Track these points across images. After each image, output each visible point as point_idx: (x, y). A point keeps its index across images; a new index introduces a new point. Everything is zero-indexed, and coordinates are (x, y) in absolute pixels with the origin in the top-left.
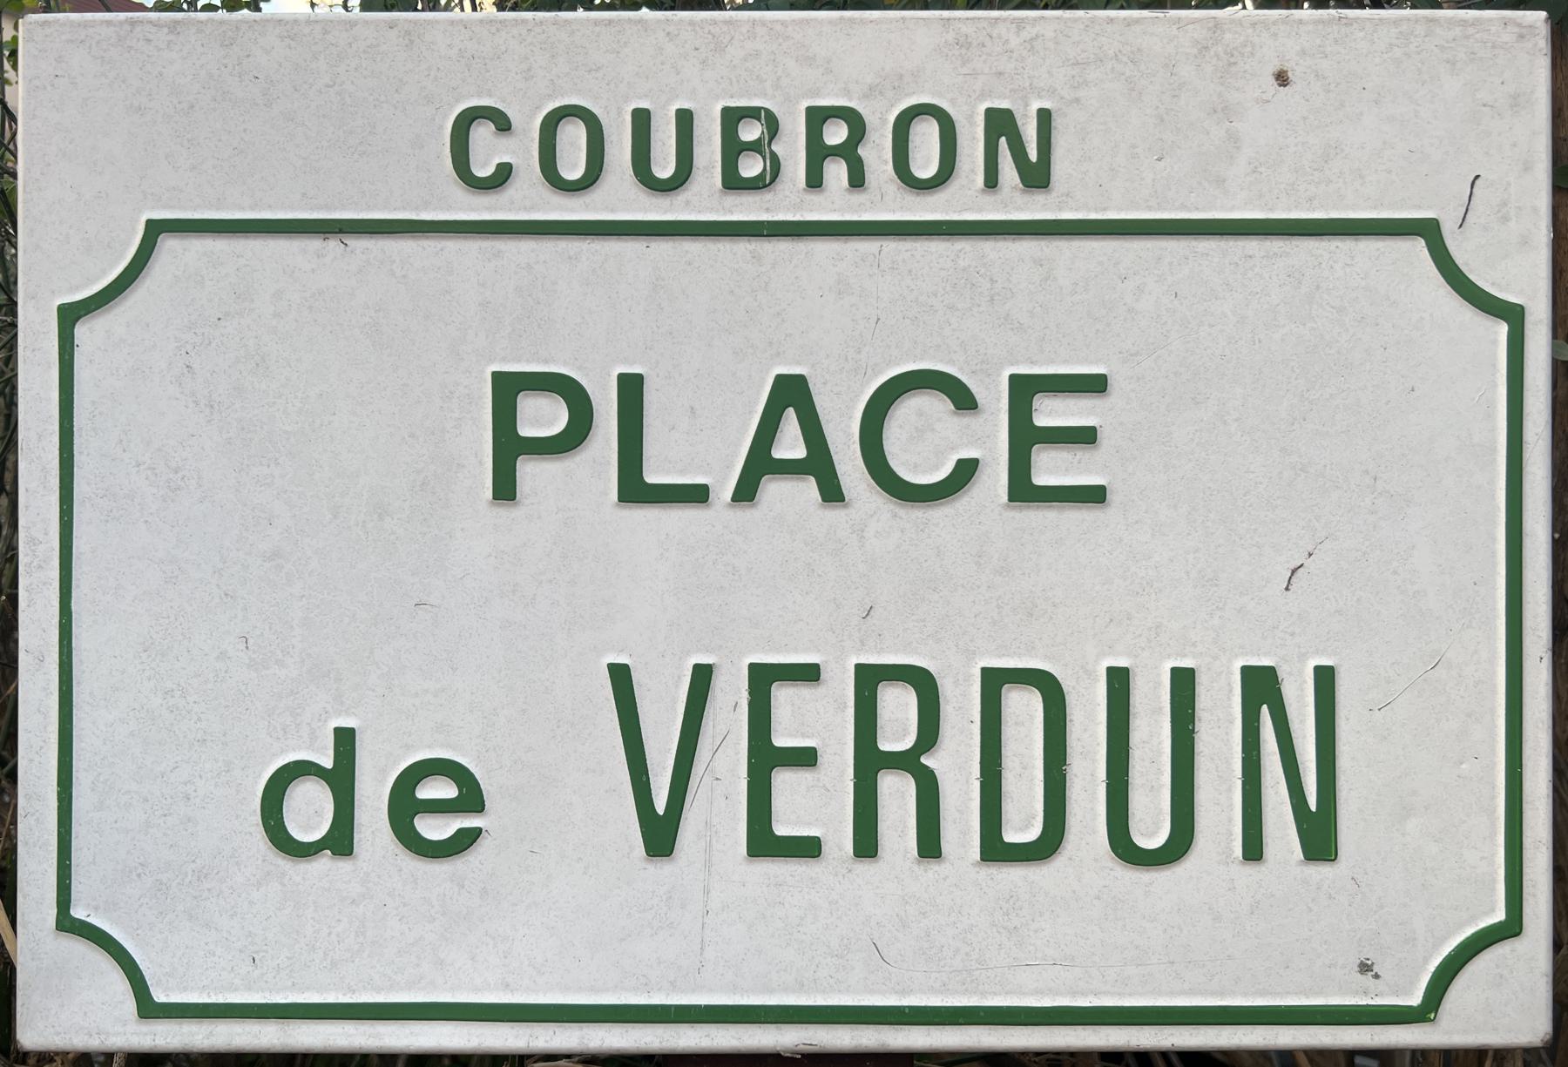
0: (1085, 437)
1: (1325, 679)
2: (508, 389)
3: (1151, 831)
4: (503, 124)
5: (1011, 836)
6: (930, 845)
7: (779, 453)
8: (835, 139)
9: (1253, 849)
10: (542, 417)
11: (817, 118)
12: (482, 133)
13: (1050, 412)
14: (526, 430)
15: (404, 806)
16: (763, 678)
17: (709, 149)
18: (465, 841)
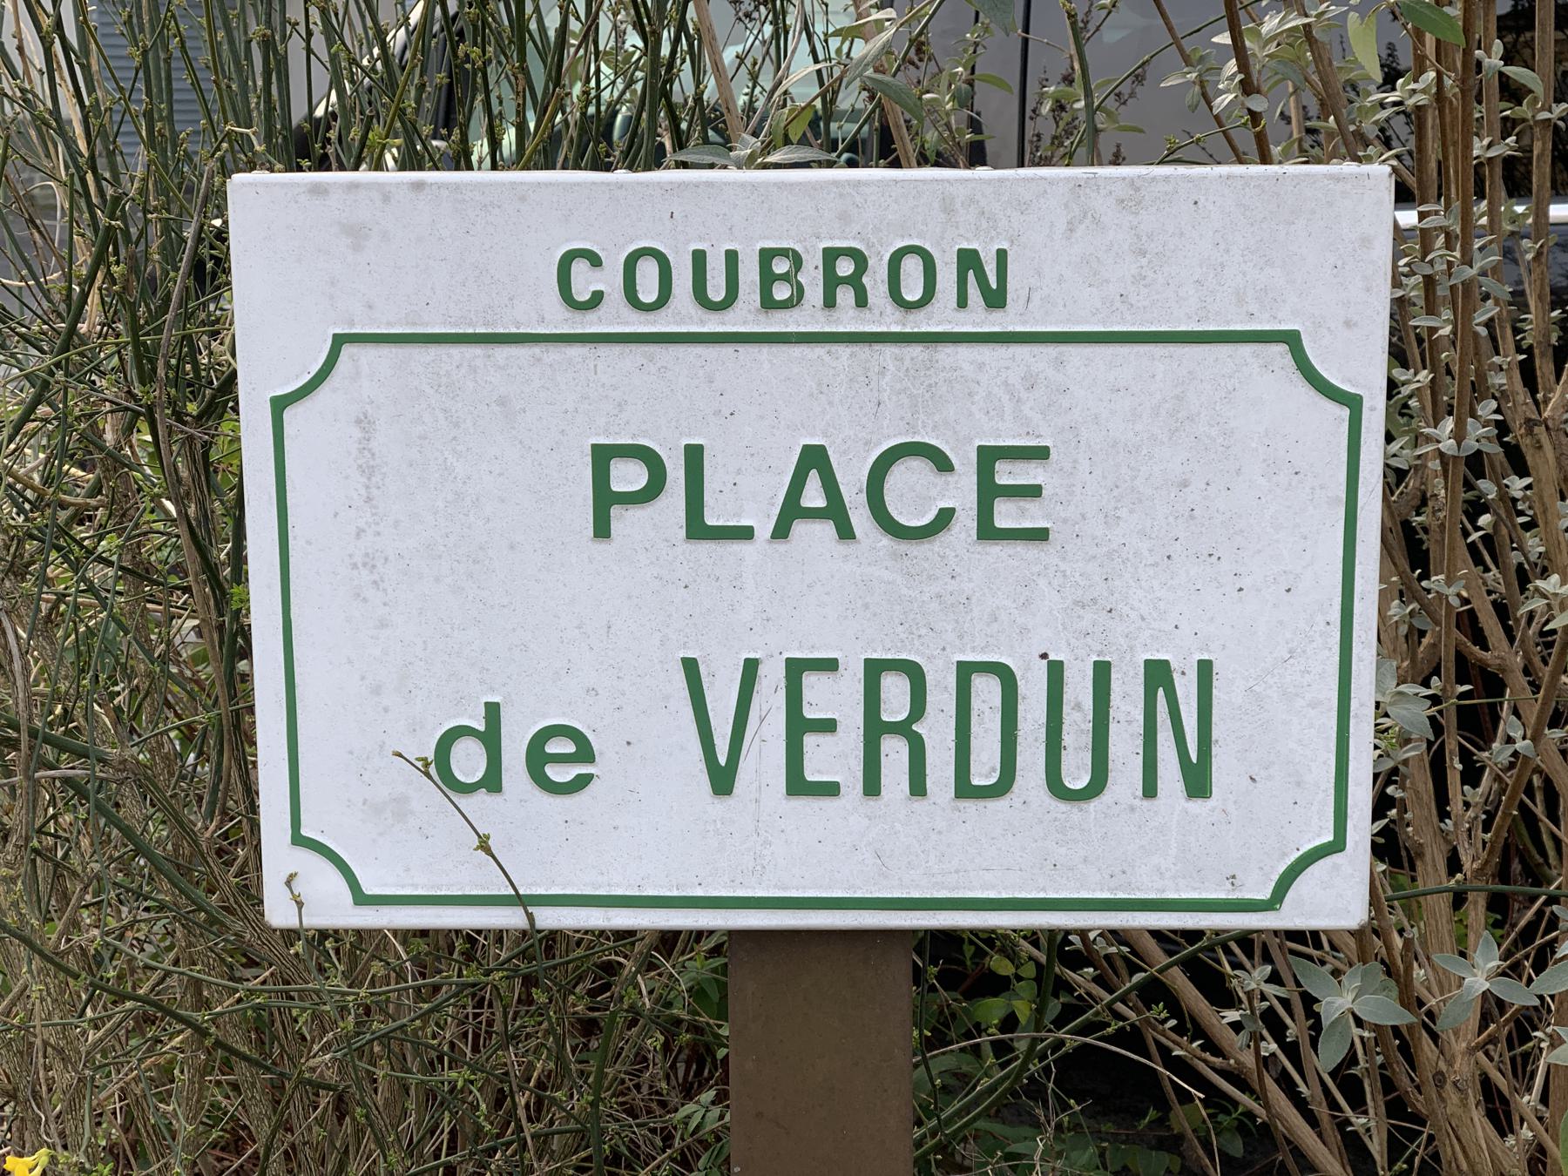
0: (1034, 492)
1: (1205, 669)
2: (603, 457)
3: (1077, 776)
4: (595, 260)
5: (976, 781)
6: (918, 787)
8: (844, 272)
9: (1150, 790)
10: (628, 476)
11: (831, 256)
12: (579, 268)
13: (1006, 474)
14: (616, 486)
15: (537, 758)
16: (796, 669)
17: (749, 274)
18: (582, 782)
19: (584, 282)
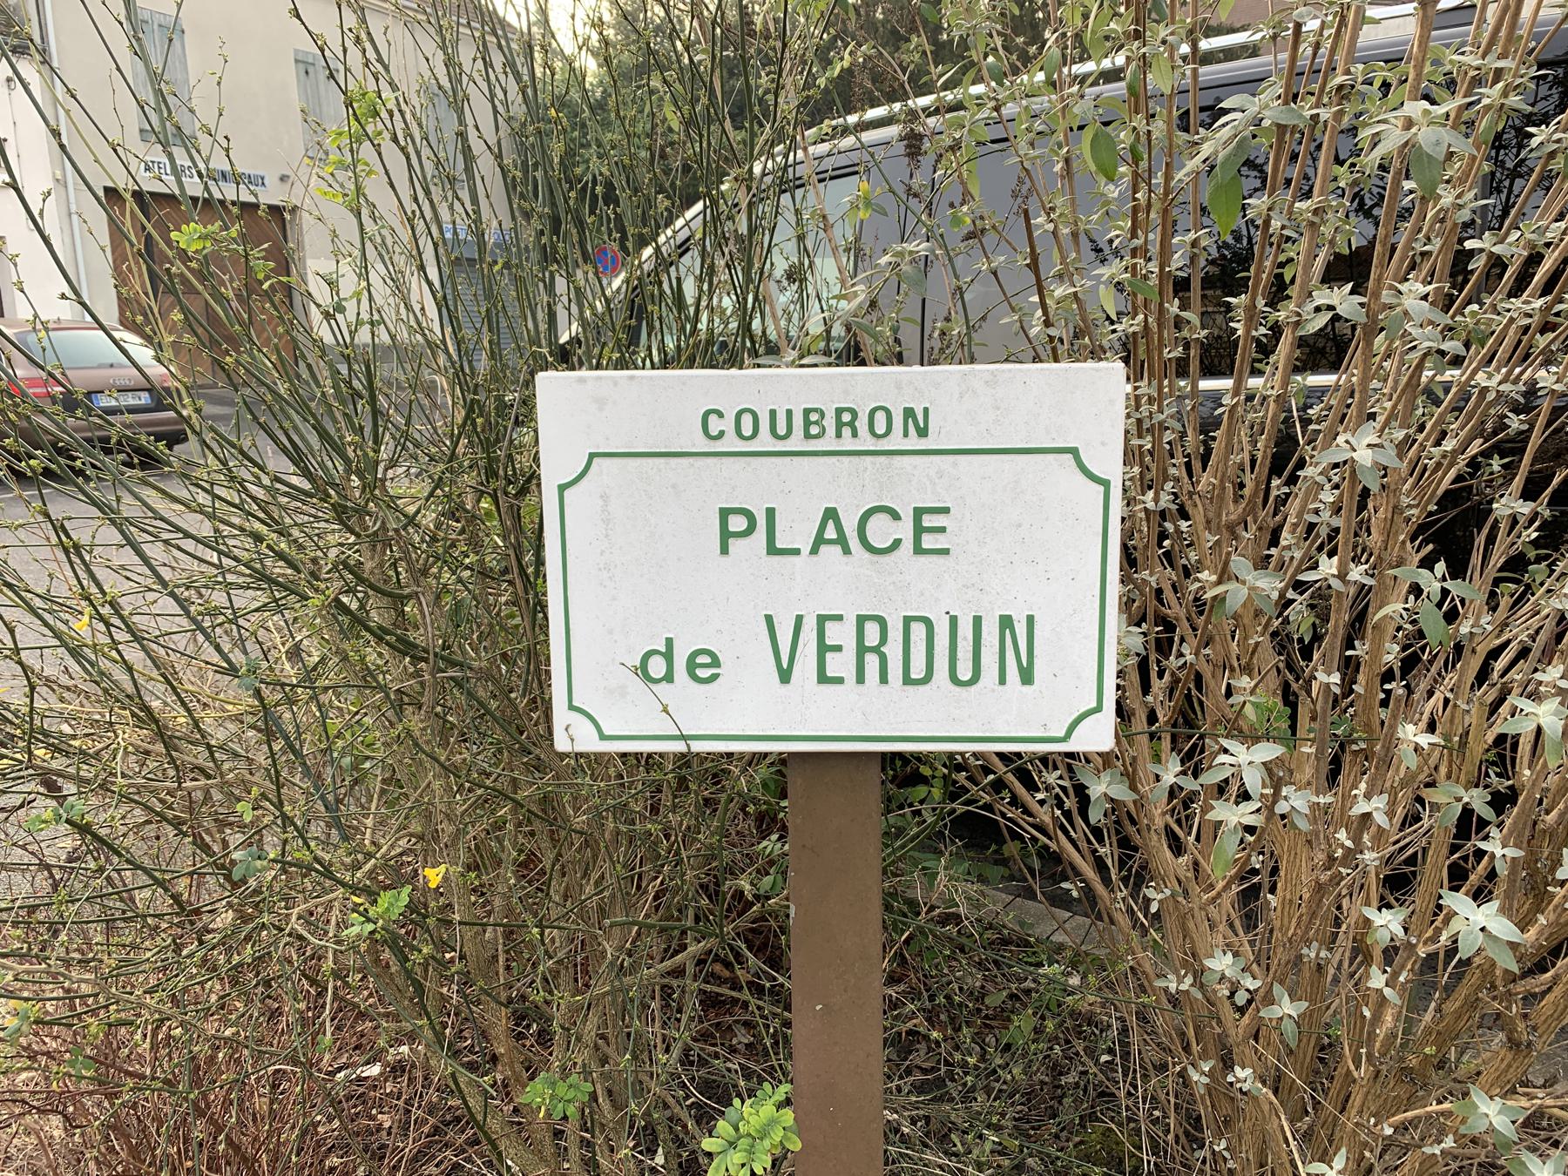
0: (942, 530)
2: (725, 513)
3: (965, 673)
4: (720, 415)
6: (884, 679)
7: (826, 536)
8: (846, 420)
9: (1002, 681)
10: (737, 523)
11: (839, 411)
12: (713, 418)
13: (928, 521)
15: (692, 666)
16: (822, 620)
17: (798, 421)
18: (714, 677)
19: (715, 425)
